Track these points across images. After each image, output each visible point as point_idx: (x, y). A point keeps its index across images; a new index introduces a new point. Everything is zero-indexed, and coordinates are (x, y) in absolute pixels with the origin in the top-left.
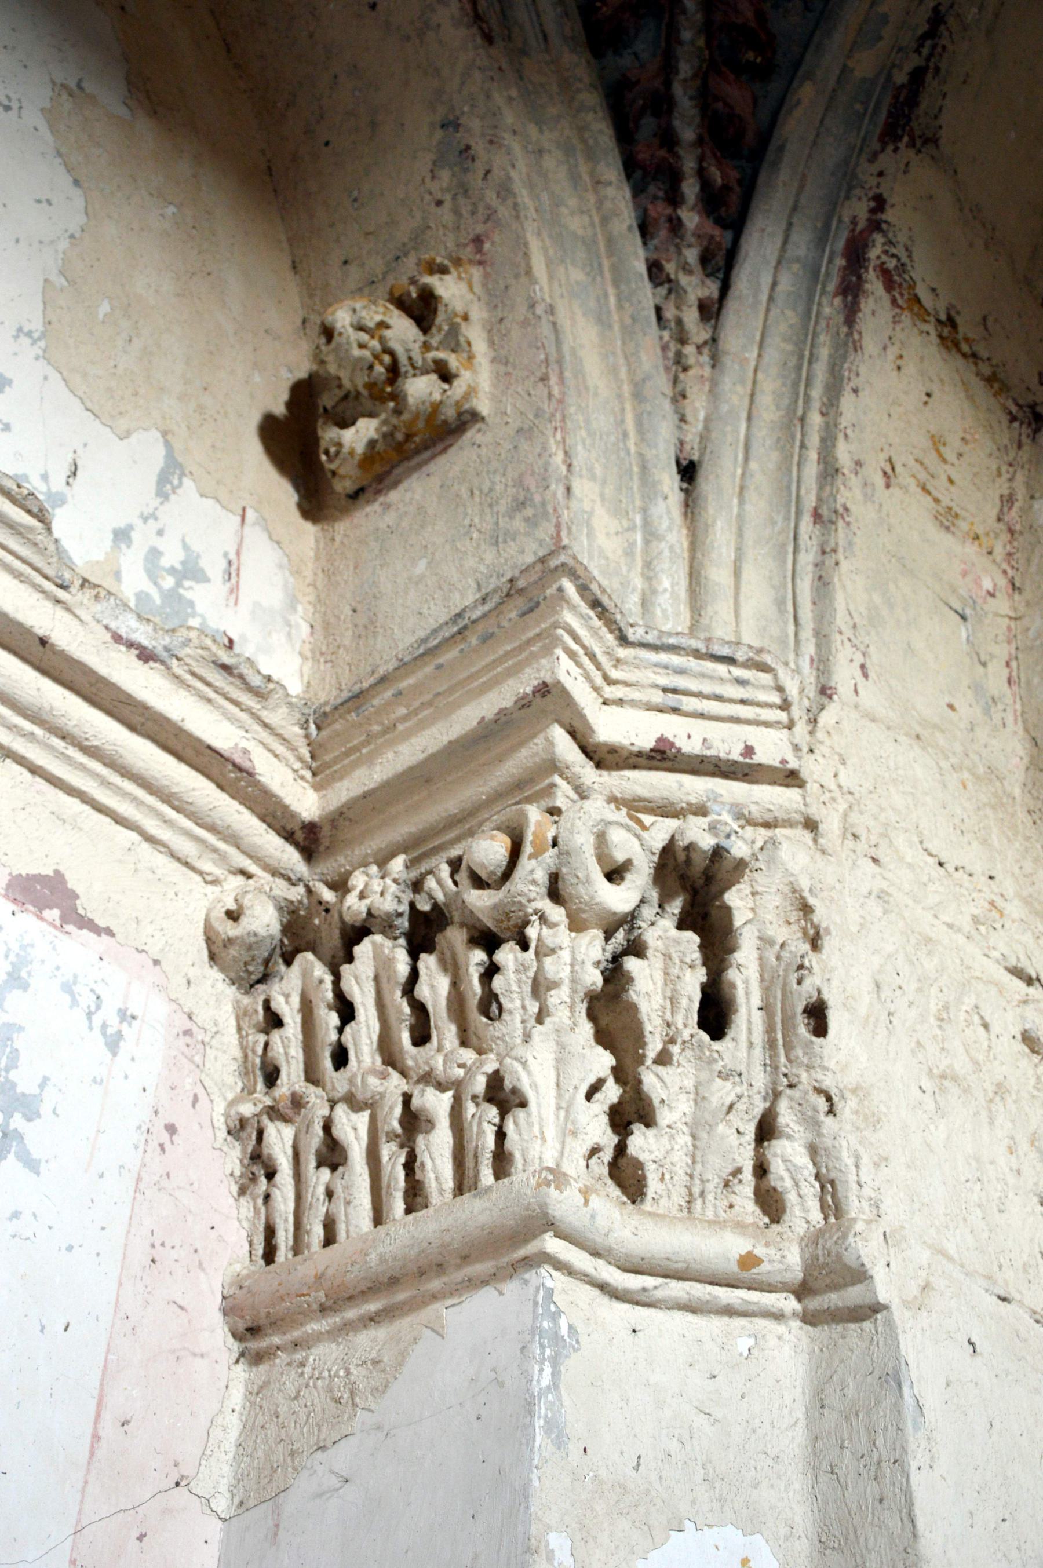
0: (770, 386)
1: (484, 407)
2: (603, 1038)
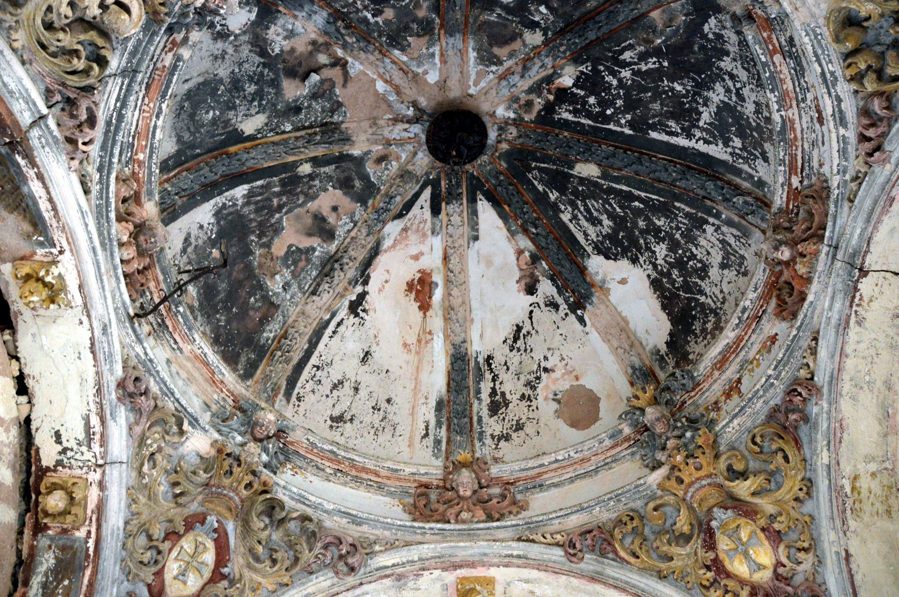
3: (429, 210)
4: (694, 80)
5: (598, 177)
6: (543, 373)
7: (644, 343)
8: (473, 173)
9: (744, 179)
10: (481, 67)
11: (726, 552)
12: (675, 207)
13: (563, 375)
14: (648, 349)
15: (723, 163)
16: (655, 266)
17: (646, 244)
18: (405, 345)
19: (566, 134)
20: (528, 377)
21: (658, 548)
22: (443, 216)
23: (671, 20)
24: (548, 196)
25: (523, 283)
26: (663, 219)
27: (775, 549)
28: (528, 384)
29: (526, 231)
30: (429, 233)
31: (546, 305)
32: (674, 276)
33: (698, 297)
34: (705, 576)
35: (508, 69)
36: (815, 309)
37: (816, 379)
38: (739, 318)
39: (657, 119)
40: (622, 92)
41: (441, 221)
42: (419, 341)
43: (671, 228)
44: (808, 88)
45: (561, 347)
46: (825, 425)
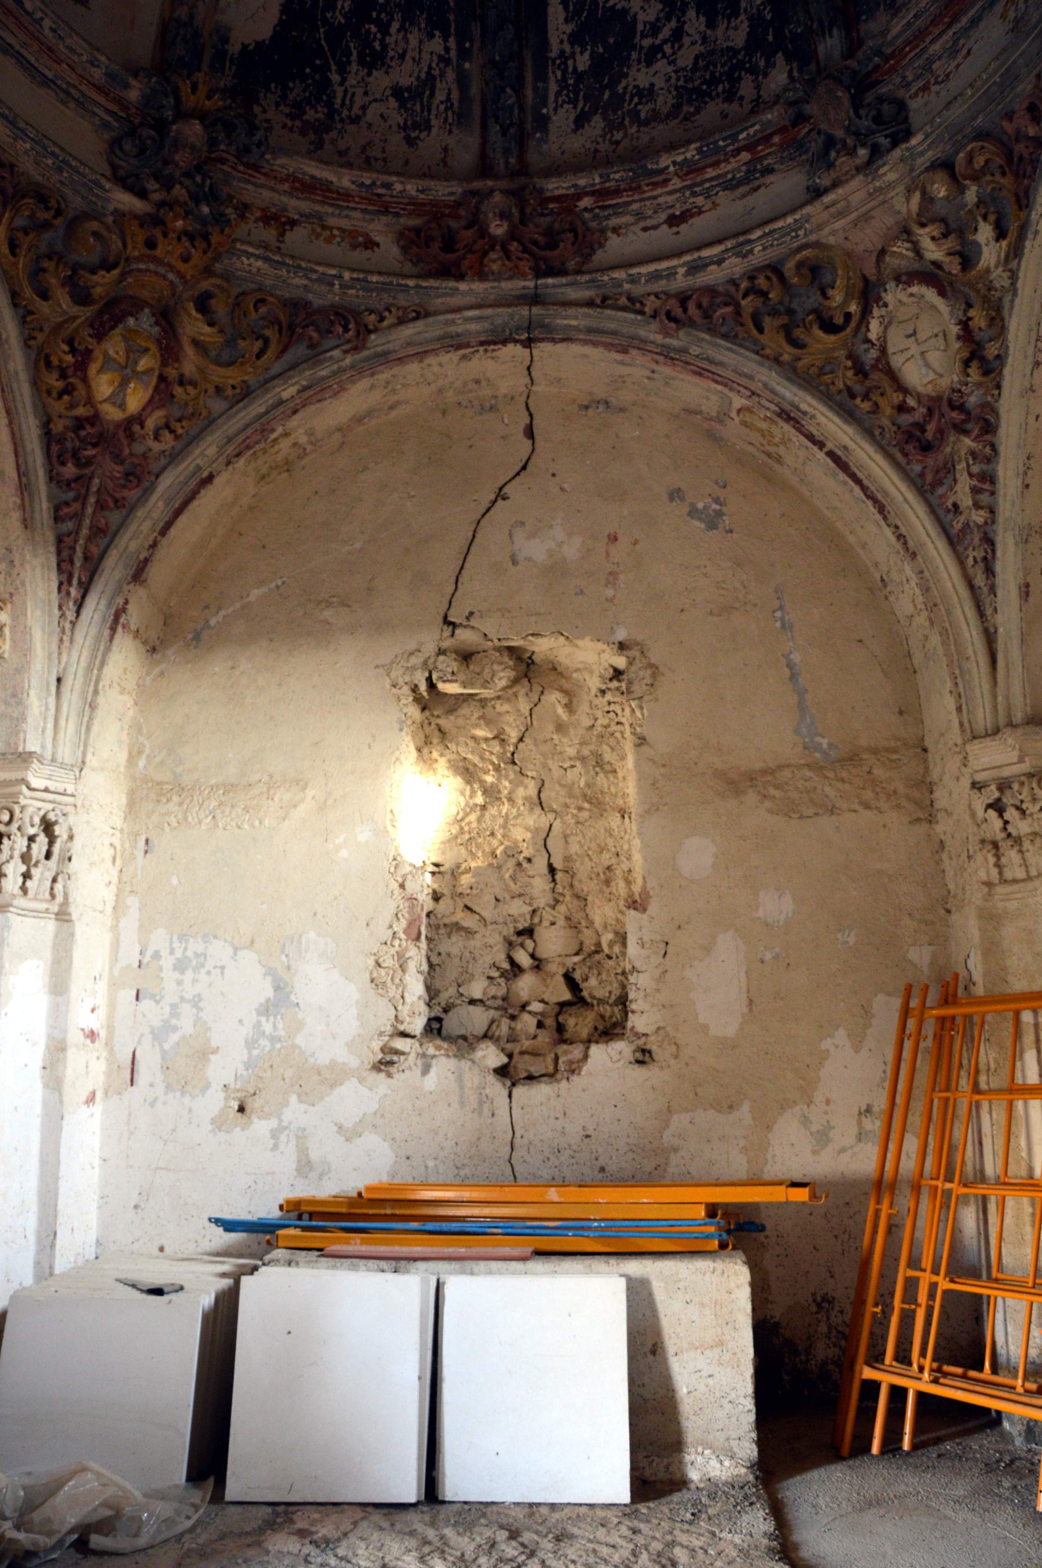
0: (85, 654)
1: (6, 656)
2: (24, 862)
9: (535, 89)
11: (106, 355)
15: (544, 44)
21: (44, 270)
27: (150, 404)
33: (334, 68)
34: (63, 355)
36: (451, 295)
37: (373, 337)
38: (374, 183)
44: (709, 197)
46: (323, 373)
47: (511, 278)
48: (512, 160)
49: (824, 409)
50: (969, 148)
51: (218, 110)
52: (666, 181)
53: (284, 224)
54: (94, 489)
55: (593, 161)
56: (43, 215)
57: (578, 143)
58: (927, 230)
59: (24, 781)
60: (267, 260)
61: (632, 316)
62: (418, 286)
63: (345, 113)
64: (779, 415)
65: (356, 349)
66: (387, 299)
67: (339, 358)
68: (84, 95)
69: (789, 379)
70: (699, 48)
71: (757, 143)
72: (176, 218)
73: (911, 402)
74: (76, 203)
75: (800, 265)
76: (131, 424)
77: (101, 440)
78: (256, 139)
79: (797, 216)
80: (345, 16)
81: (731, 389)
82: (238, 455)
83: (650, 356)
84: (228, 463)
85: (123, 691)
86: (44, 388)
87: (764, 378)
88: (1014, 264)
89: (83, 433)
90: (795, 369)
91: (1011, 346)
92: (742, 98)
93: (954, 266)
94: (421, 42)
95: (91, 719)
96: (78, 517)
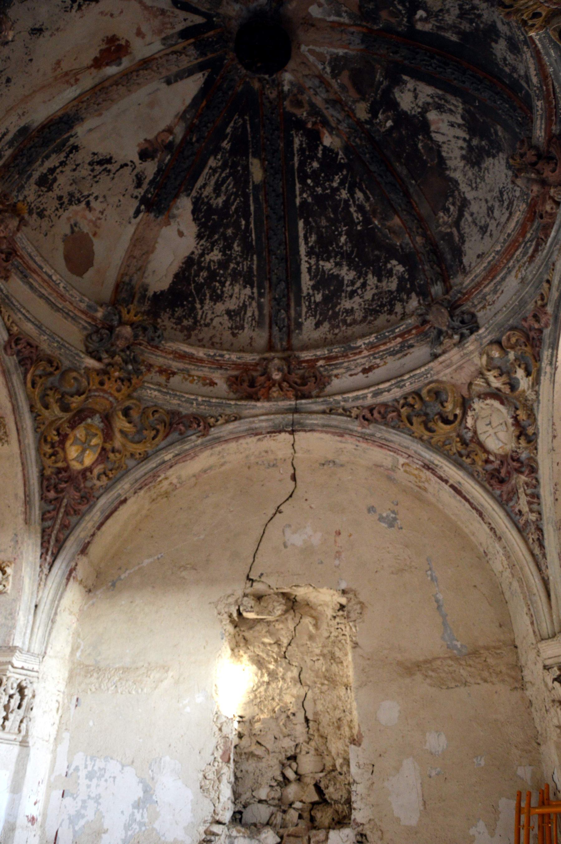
0: (52, 592)
1: (9, 592)
3: (185, 27)
4: (352, 252)
5: (253, 183)
6: (84, 203)
7: (146, 275)
8: (225, 59)
9: (296, 310)
10: (328, 57)
11: (75, 436)
12: (252, 256)
13: (91, 221)
14: (144, 280)
15: (300, 289)
16: (202, 255)
17: (216, 241)
18: (58, 63)
19: (282, 145)
20: (76, 192)
21: (48, 395)
22: (182, 44)
23: (394, 232)
24: (224, 140)
25: (147, 145)
26: (239, 249)
27: (96, 462)
28: (71, 195)
29: (190, 129)
30: (163, 35)
31: (137, 176)
32: (201, 274)
33: (198, 301)
35: (329, 84)
36: (253, 409)
37: (212, 429)
38: (215, 355)
39: (314, 224)
40: (328, 191)
41: (176, 44)
42: (66, 74)
43: (236, 258)
45: (110, 206)
46: (187, 447)
47: (283, 400)
48: (284, 343)
49: (447, 463)
50: (508, 333)
51: (140, 321)
52: (360, 352)
53: (170, 374)
54: (64, 504)
55: (325, 343)
56: (51, 369)
57: (317, 335)
58: (491, 373)
59: (10, 663)
60: (159, 391)
61: (345, 418)
62: (236, 404)
63: (202, 322)
64: (423, 467)
65: (203, 435)
66: (220, 410)
67: (194, 440)
68: (76, 315)
69: (427, 448)
70: (374, 291)
71: (405, 333)
72: (115, 371)
73: (492, 458)
74: (67, 363)
75: (429, 391)
76: (85, 472)
77: (70, 479)
78: (157, 334)
79: (426, 368)
80: (204, 279)
81: (398, 454)
82: (140, 489)
83: (355, 438)
84: (135, 493)
85: (71, 613)
86: (42, 452)
87: (415, 448)
88: (536, 388)
89: (60, 476)
90: (430, 443)
91: (540, 428)
92: (396, 313)
93: (506, 390)
94: (240, 290)
95: (52, 628)
96: (54, 519)
